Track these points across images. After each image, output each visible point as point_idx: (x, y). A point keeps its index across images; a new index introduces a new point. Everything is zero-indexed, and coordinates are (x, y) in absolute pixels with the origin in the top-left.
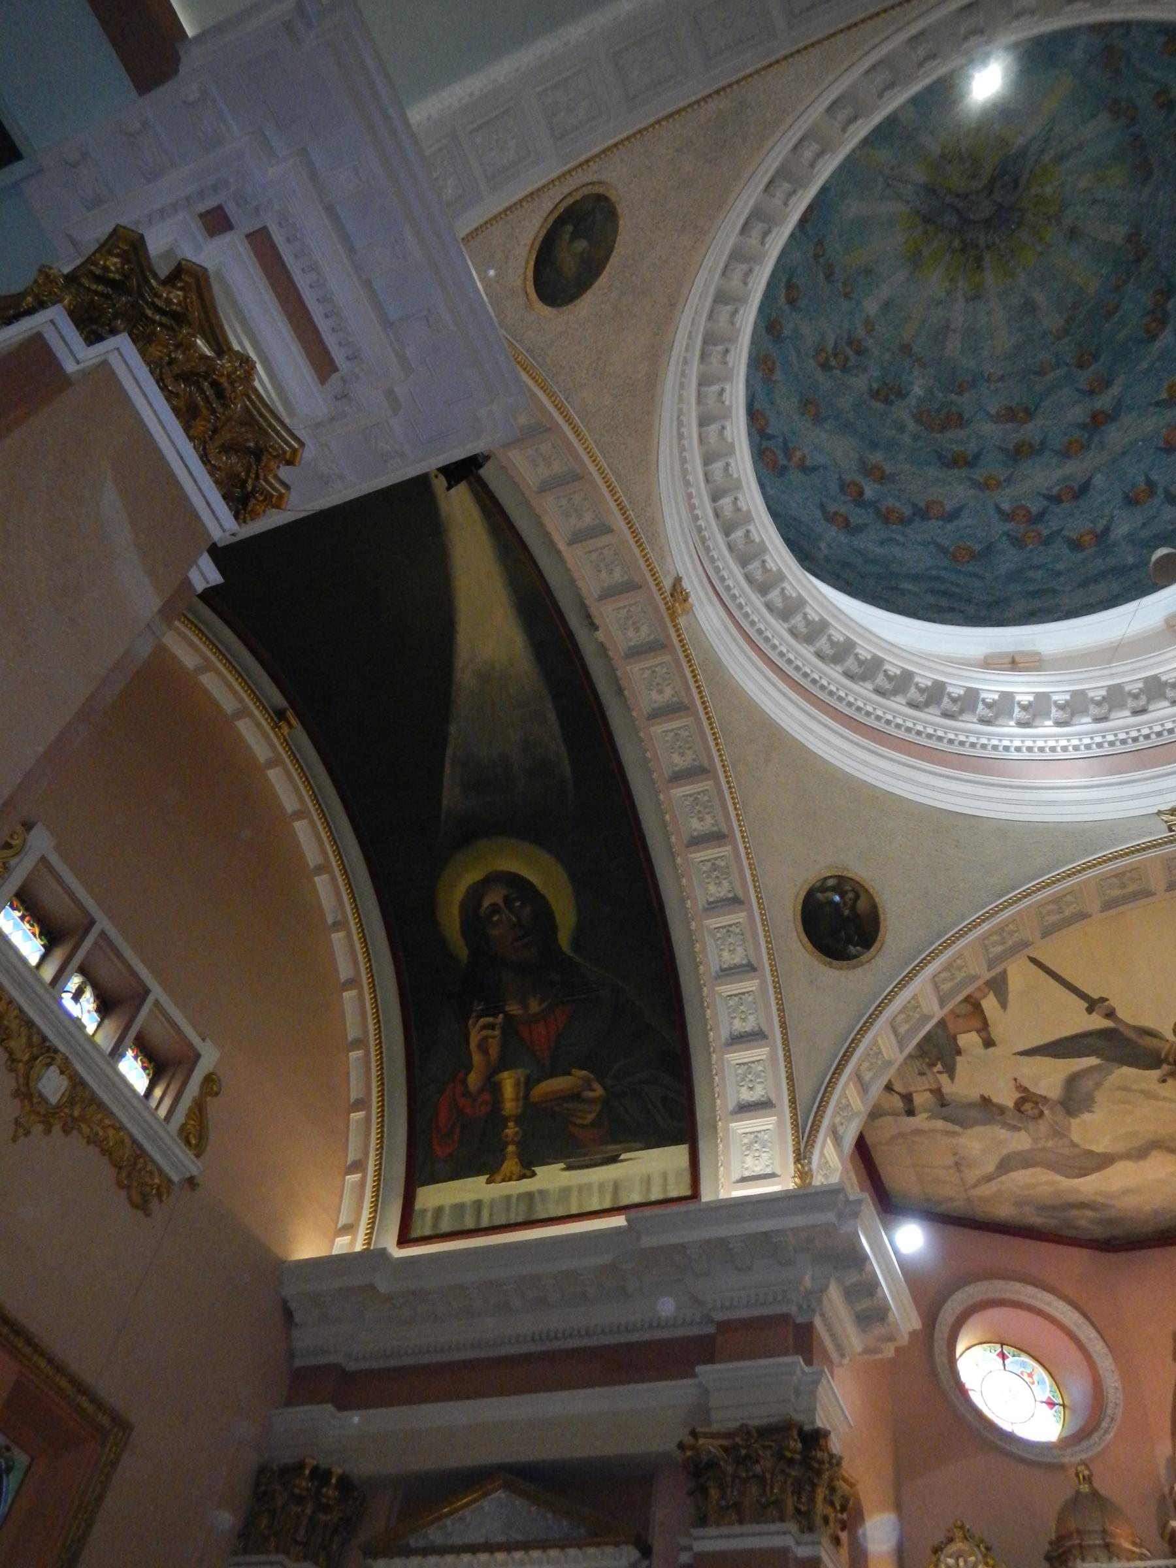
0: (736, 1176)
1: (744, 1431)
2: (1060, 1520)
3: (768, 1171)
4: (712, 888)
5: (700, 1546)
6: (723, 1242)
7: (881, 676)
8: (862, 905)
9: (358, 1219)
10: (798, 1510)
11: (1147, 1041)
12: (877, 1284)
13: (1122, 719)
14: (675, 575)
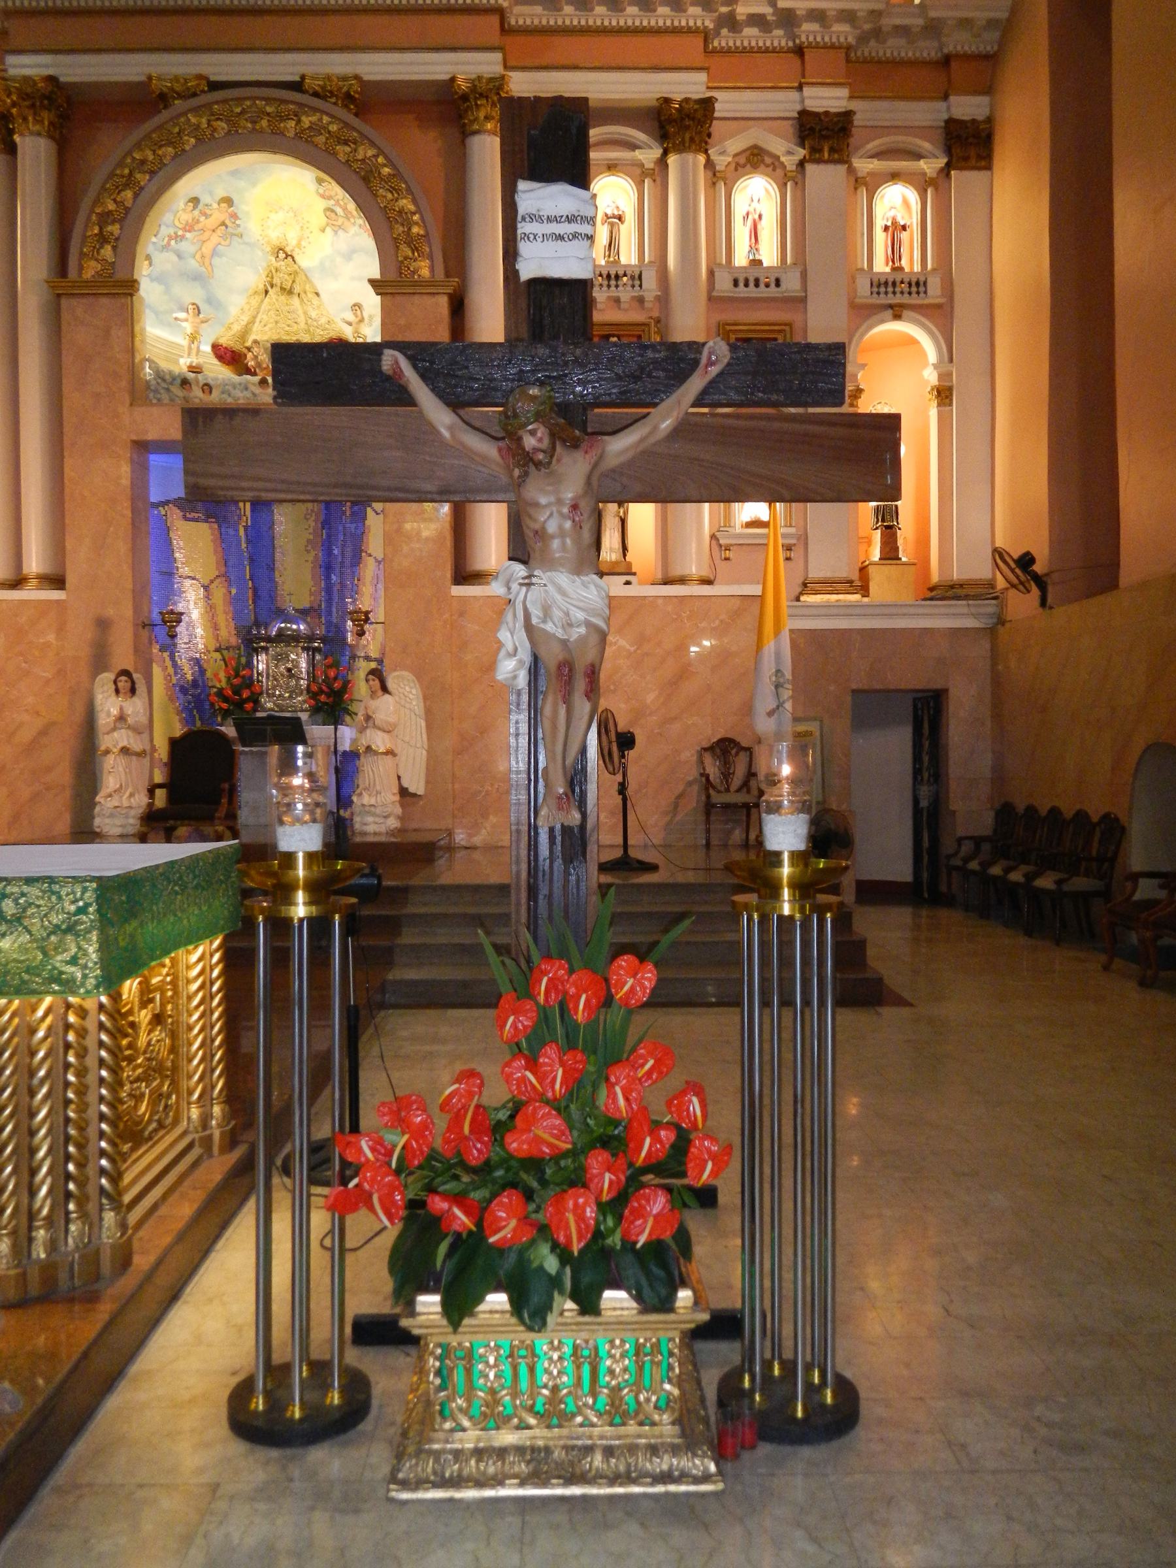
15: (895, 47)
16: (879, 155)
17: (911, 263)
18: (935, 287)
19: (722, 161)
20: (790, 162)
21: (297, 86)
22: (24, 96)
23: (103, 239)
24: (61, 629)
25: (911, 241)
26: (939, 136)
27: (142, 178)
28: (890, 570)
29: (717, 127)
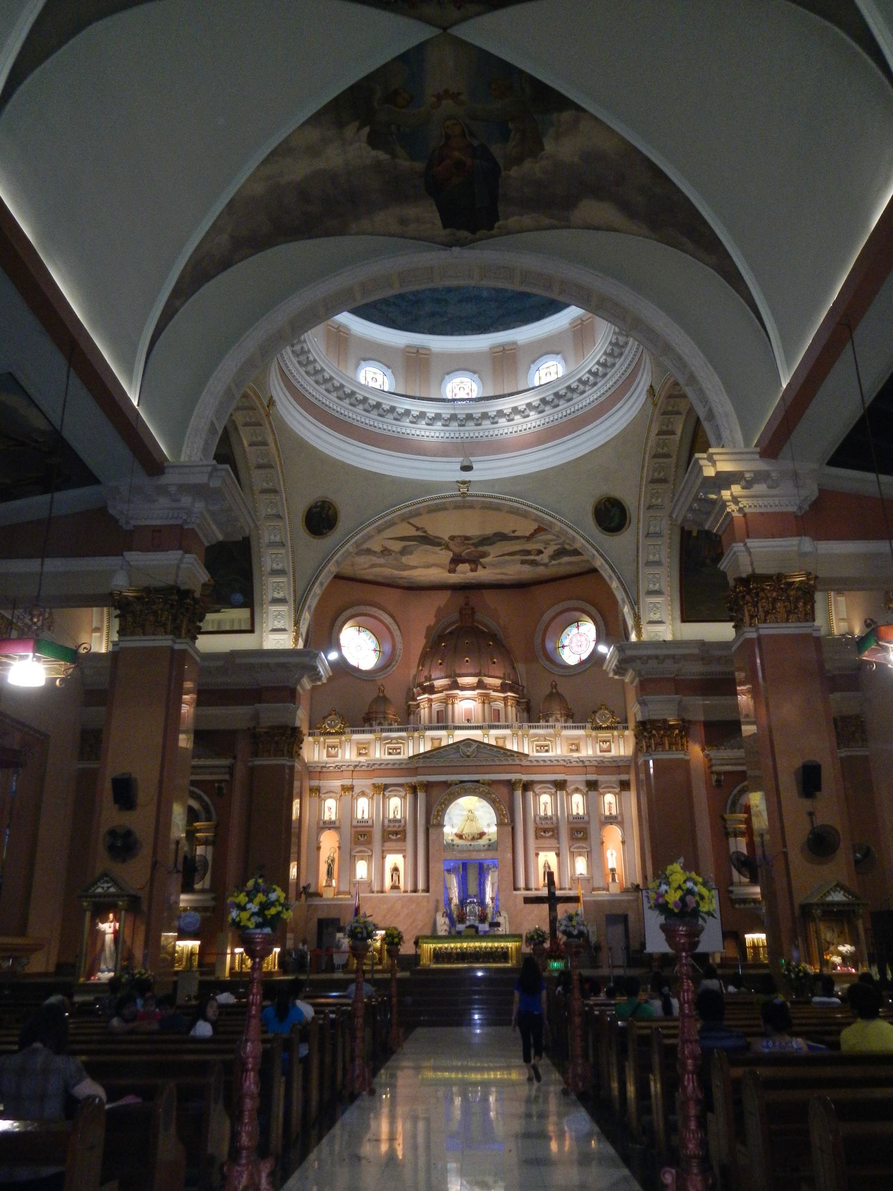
0: (270, 628)
1: (272, 728)
2: (370, 706)
3: (283, 627)
4: (269, 510)
5: (257, 762)
6: (268, 664)
7: (354, 398)
8: (331, 512)
9: (102, 626)
10: (288, 751)
11: (437, 540)
12: (320, 672)
13: (454, 425)
14: (270, 395)
15: (607, 764)
16: (604, 788)
17: (614, 813)
18: (619, 818)
19: (569, 792)
20: (585, 791)
21: (478, 781)
22: (421, 785)
23: (438, 815)
24: (428, 902)
25: (614, 806)
26: (618, 783)
27: (446, 802)
28: (614, 884)
29: (568, 784)
